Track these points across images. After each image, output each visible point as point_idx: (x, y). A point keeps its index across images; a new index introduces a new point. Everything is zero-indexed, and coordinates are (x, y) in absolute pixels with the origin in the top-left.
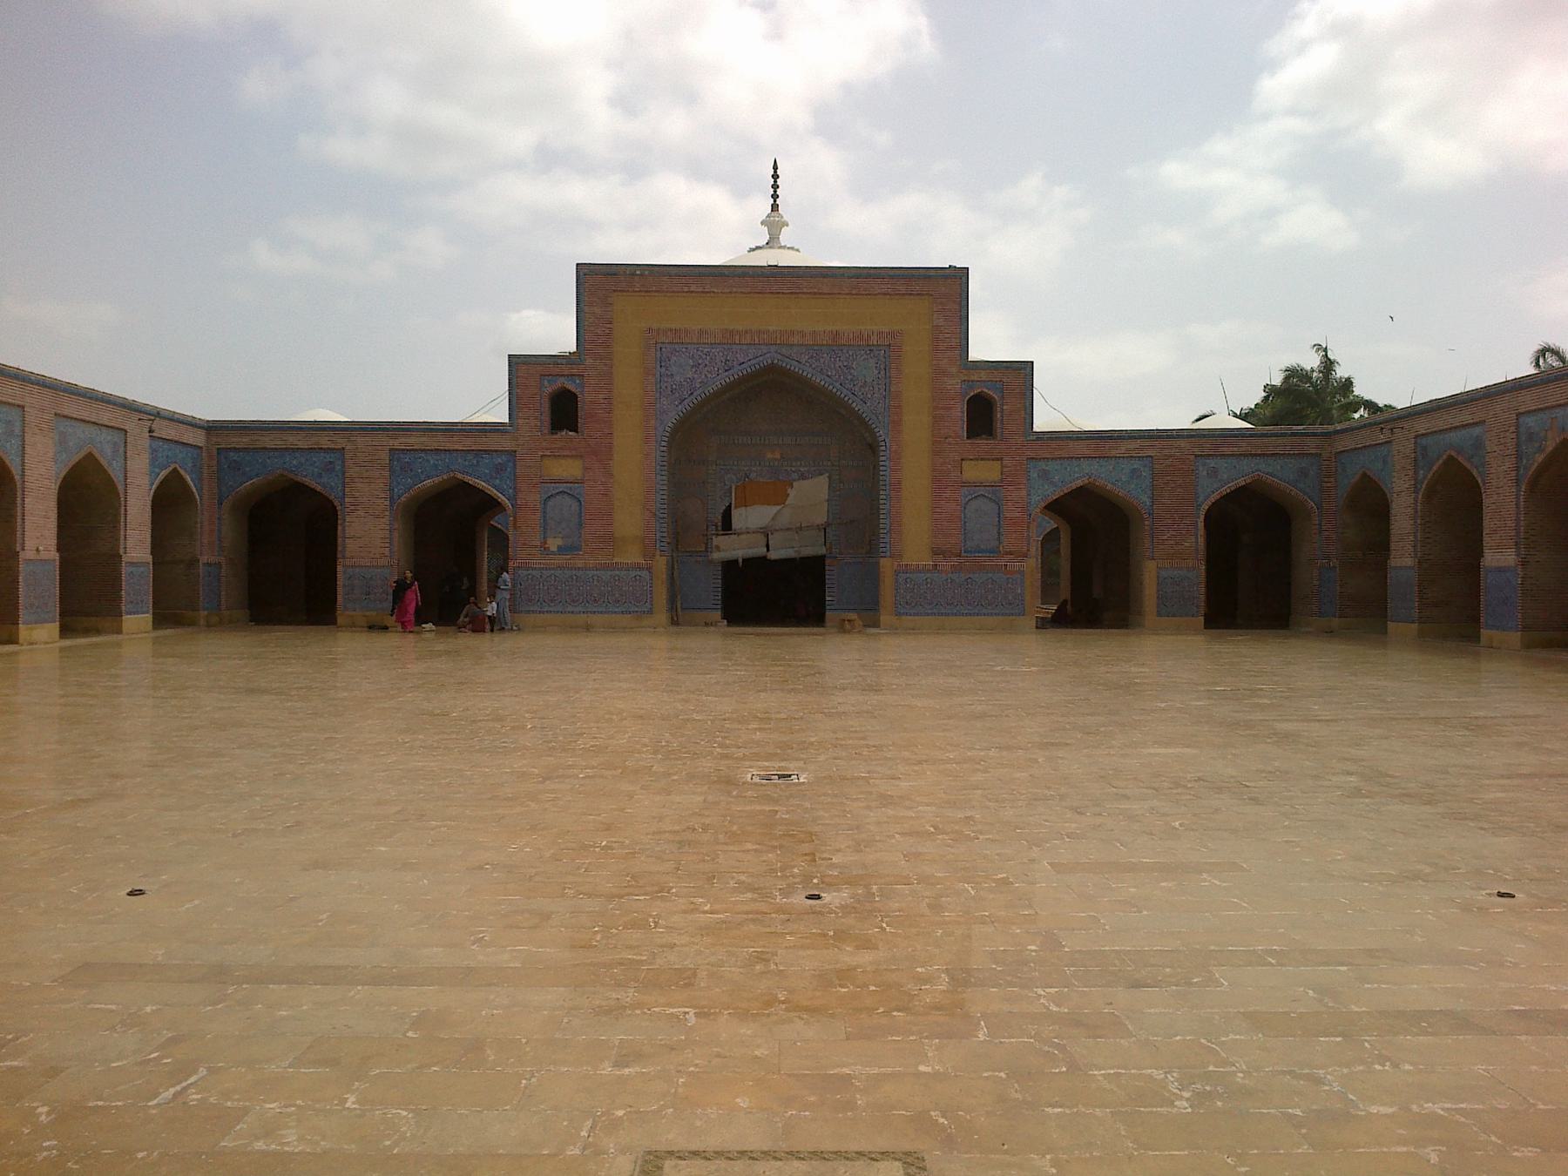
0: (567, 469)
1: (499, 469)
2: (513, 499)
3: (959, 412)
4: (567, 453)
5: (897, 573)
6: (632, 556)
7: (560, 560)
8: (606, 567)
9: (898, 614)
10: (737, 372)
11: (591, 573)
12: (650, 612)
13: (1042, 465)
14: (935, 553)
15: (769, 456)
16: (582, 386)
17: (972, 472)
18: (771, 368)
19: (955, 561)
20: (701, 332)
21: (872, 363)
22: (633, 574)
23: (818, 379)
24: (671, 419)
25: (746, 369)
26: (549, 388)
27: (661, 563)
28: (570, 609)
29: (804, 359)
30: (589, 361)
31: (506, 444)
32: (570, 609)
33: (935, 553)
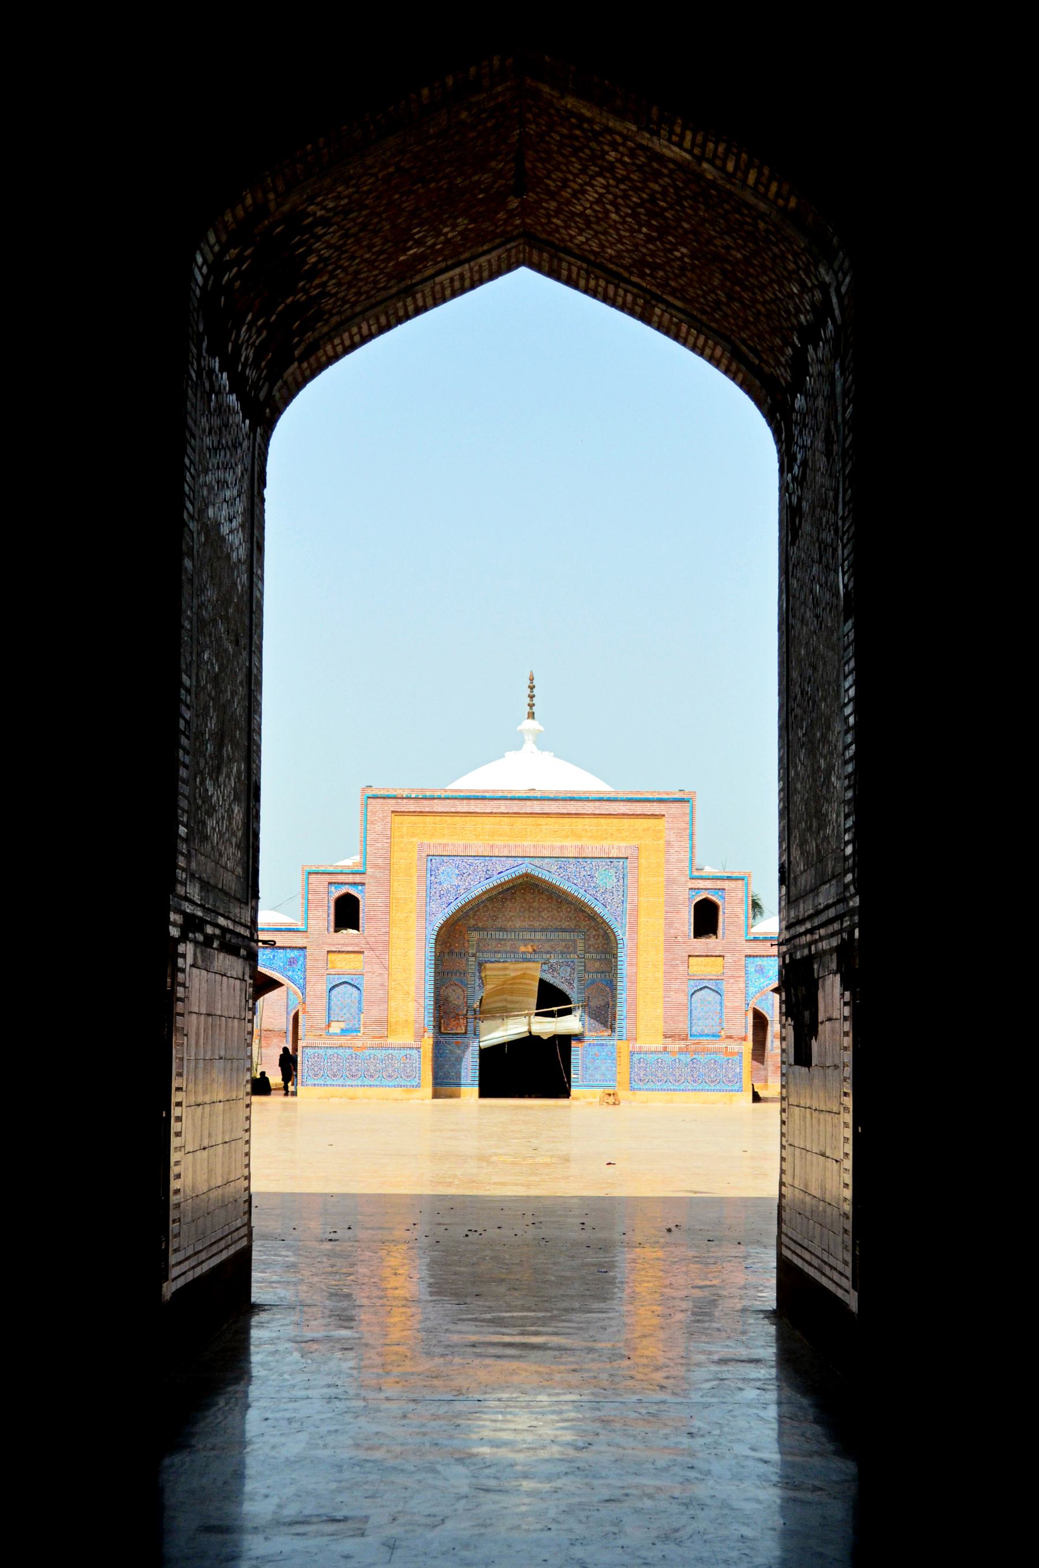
0: (346, 964)
1: (292, 962)
2: (303, 988)
3: (687, 918)
4: (350, 949)
5: (632, 1053)
6: (404, 1038)
7: (342, 1041)
8: (381, 1047)
9: (632, 1089)
10: (495, 881)
11: (367, 1052)
12: (418, 1086)
13: (758, 961)
14: (666, 1036)
15: (522, 949)
16: (362, 891)
17: (698, 967)
18: (526, 875)
19: (682, 1044)
20: (466, 847)
21: (613, 871)
22: (403, 1052)
23: (565, 886)
24: (439, 920)
25: (505, 877)
26: (338, 892)
27: (428, 1042)
28: (349, 1082)
29: (554, 868)
30: (369, 871)
31: (298, 941)
32: (349, 1082)
33: (666, 1036)
